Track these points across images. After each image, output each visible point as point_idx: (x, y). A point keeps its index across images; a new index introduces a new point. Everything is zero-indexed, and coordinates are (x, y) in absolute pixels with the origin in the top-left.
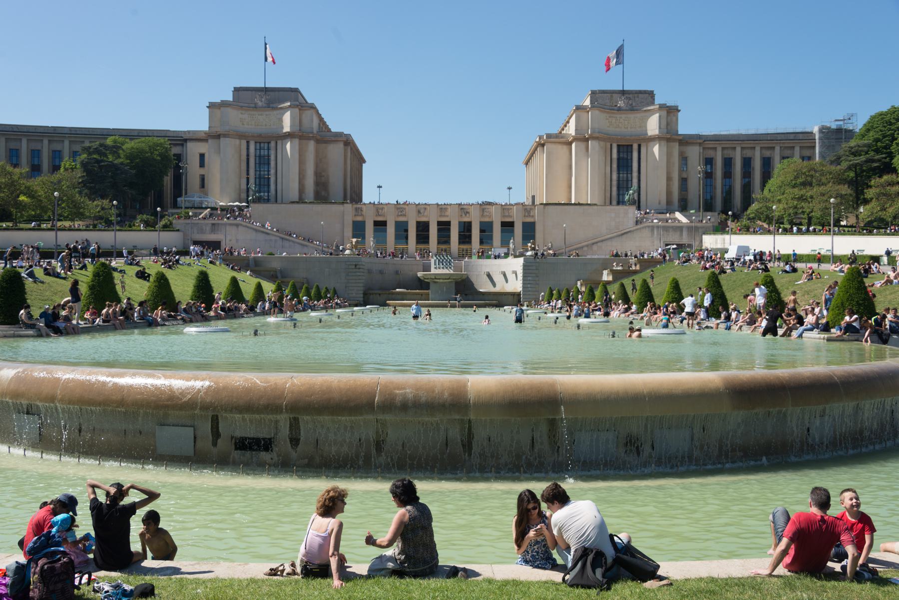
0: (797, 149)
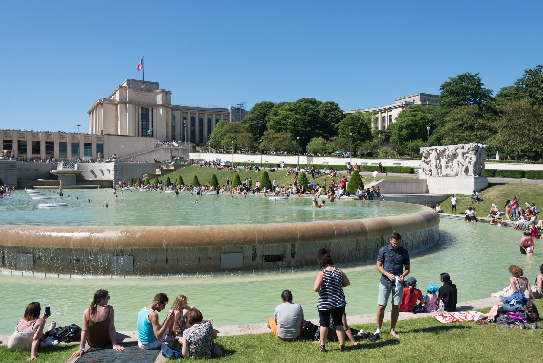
0: (222, 116)
